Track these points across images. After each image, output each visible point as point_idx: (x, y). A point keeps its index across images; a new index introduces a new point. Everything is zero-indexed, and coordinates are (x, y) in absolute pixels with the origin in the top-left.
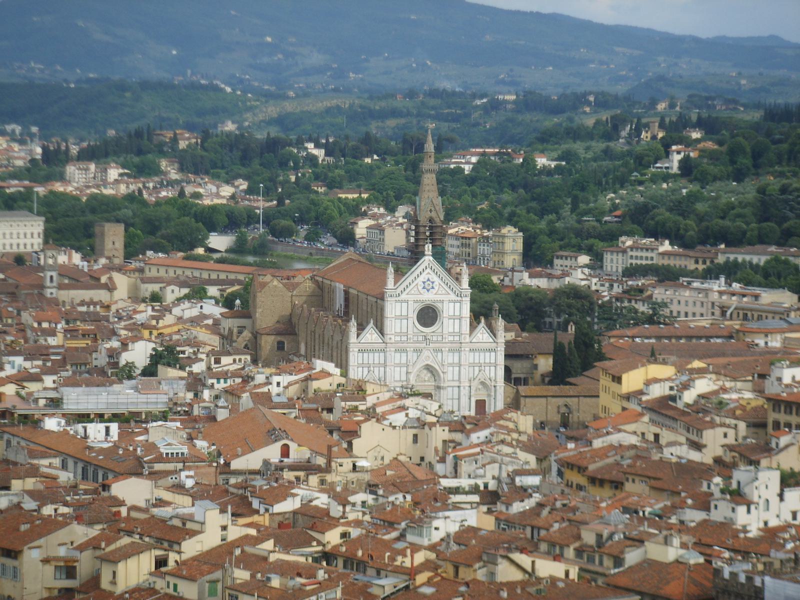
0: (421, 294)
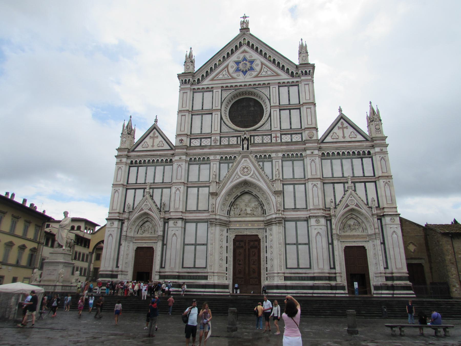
0: (233, 78)
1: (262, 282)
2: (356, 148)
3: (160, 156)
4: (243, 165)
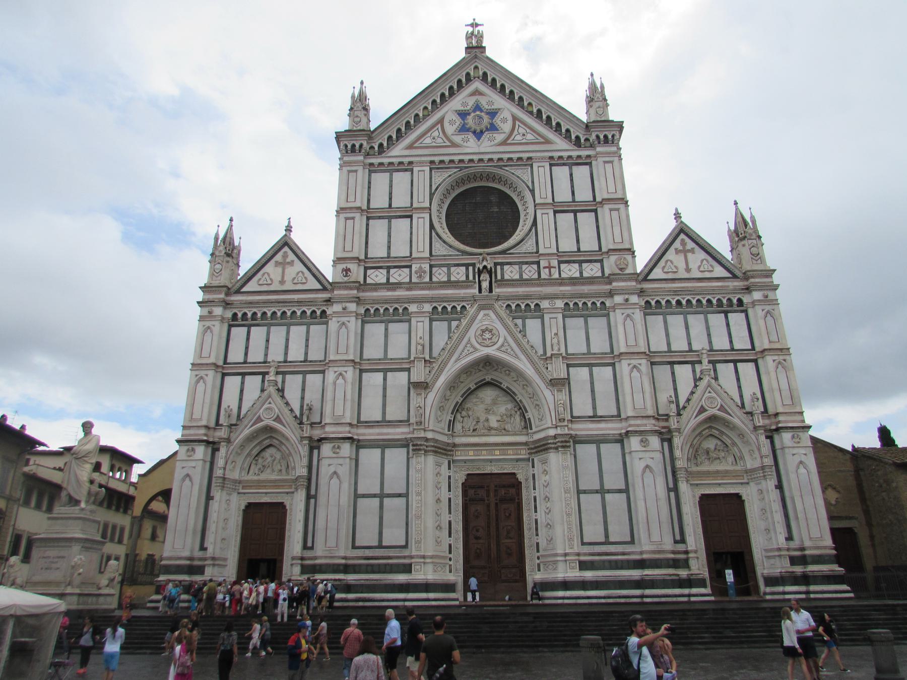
1: (529, 573)
2: (713, 291)
3: (300, 303)
4: (481, 324)
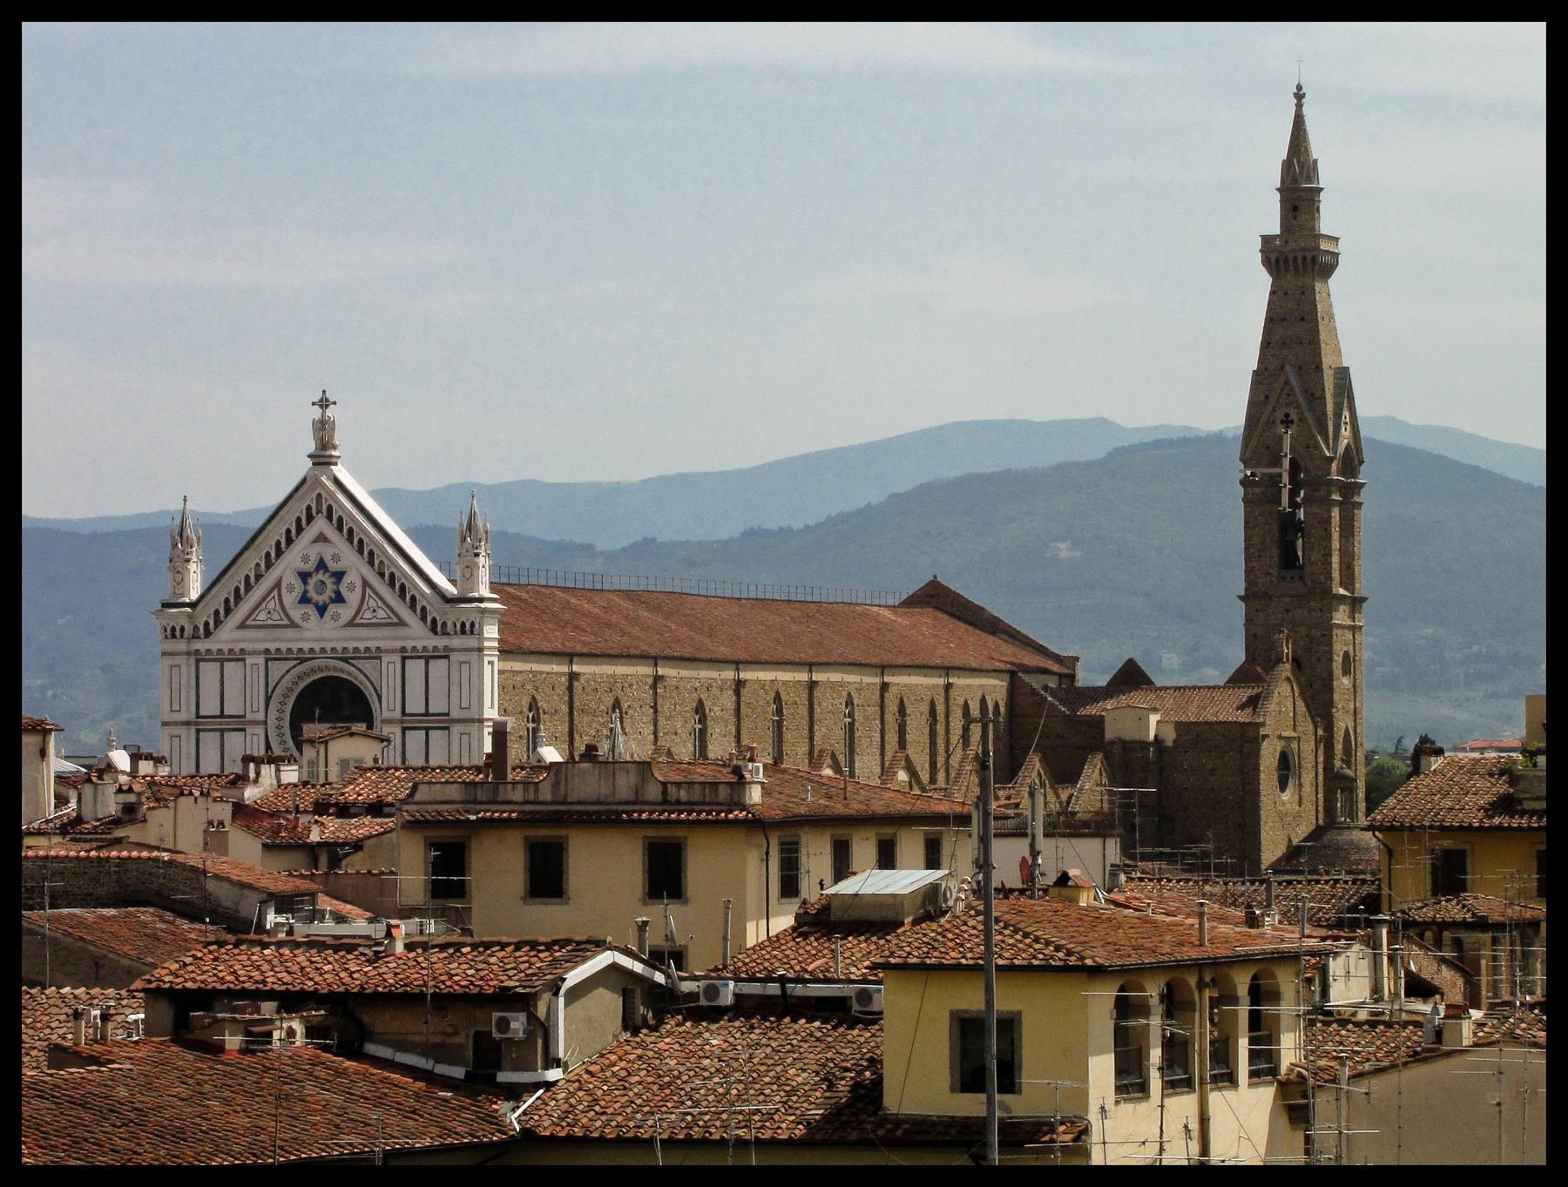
0: (293, 625)
